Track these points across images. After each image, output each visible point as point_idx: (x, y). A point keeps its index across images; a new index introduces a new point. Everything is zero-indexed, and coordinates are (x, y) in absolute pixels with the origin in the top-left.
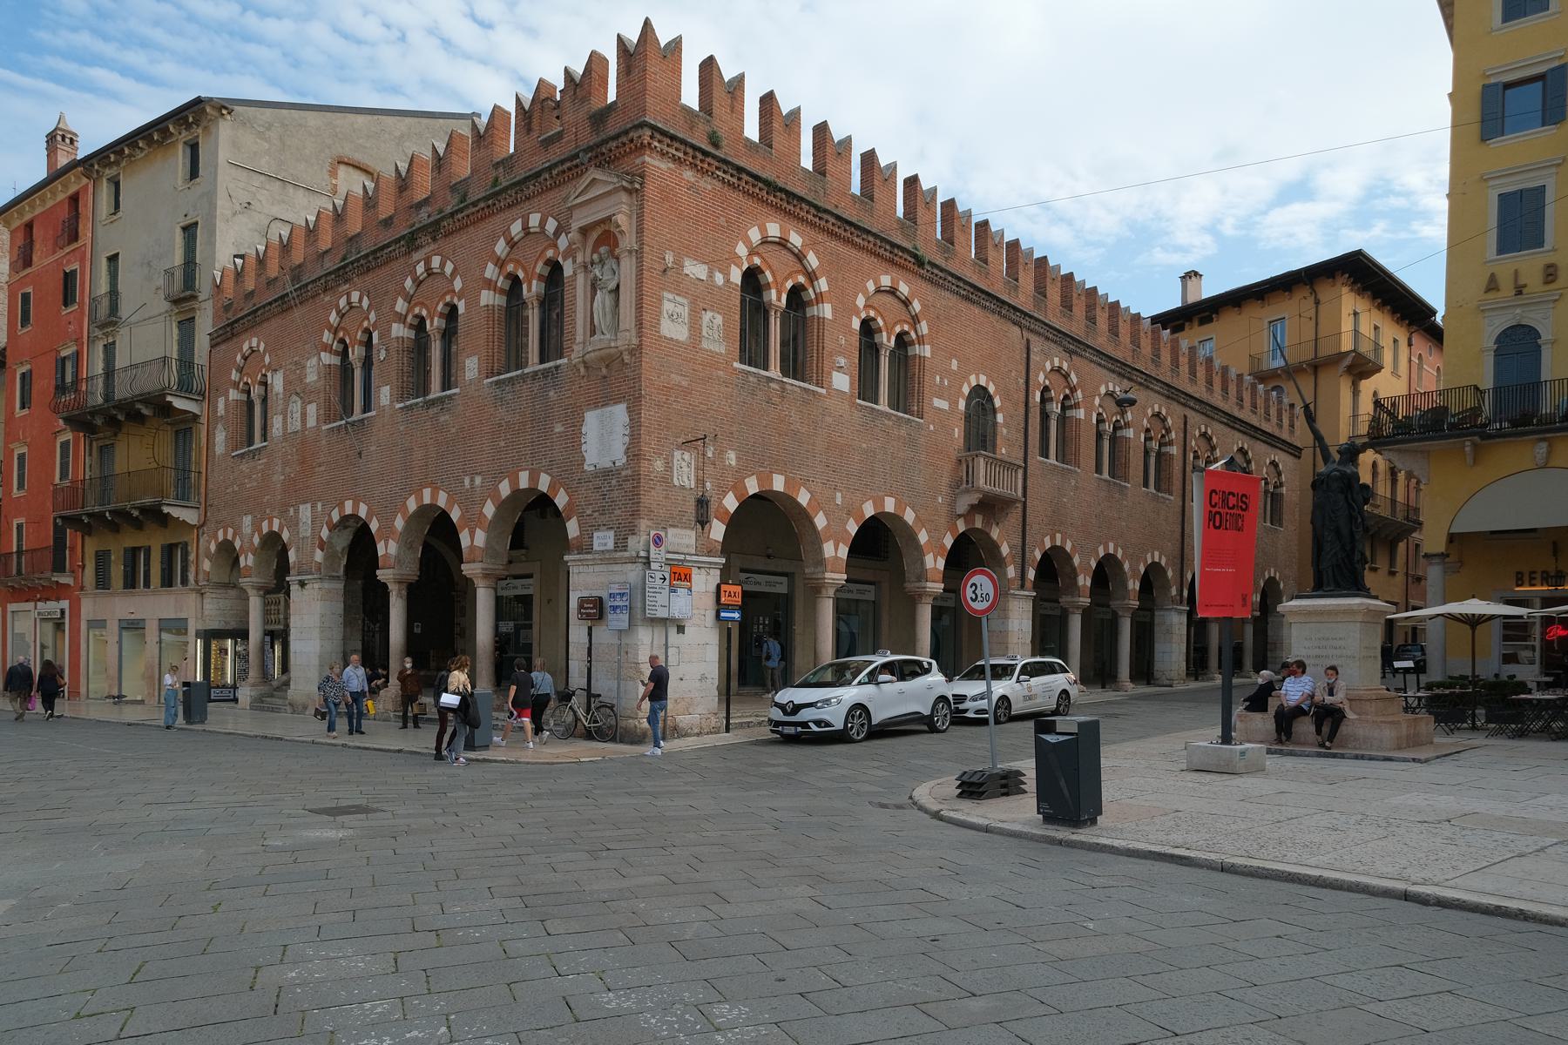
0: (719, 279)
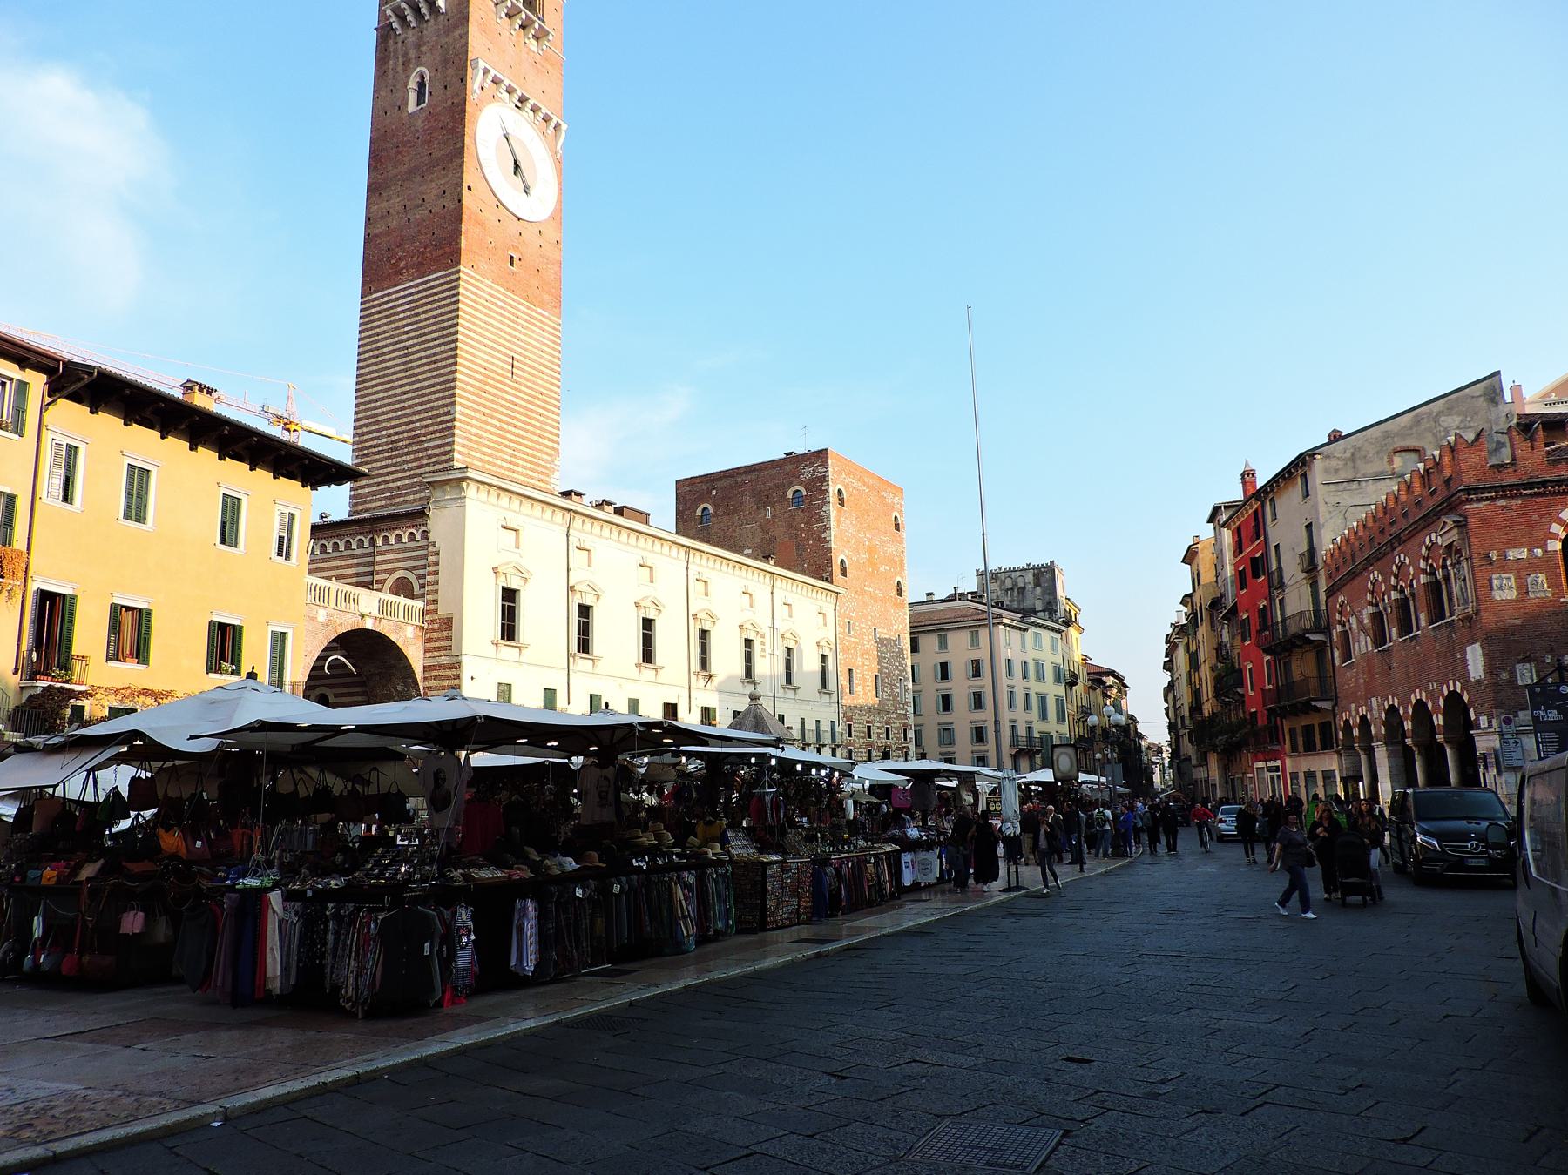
0: (1539, 552)
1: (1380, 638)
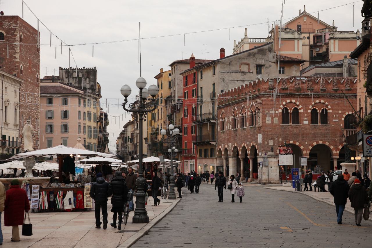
0: (277, 112)
1: (234, 126)
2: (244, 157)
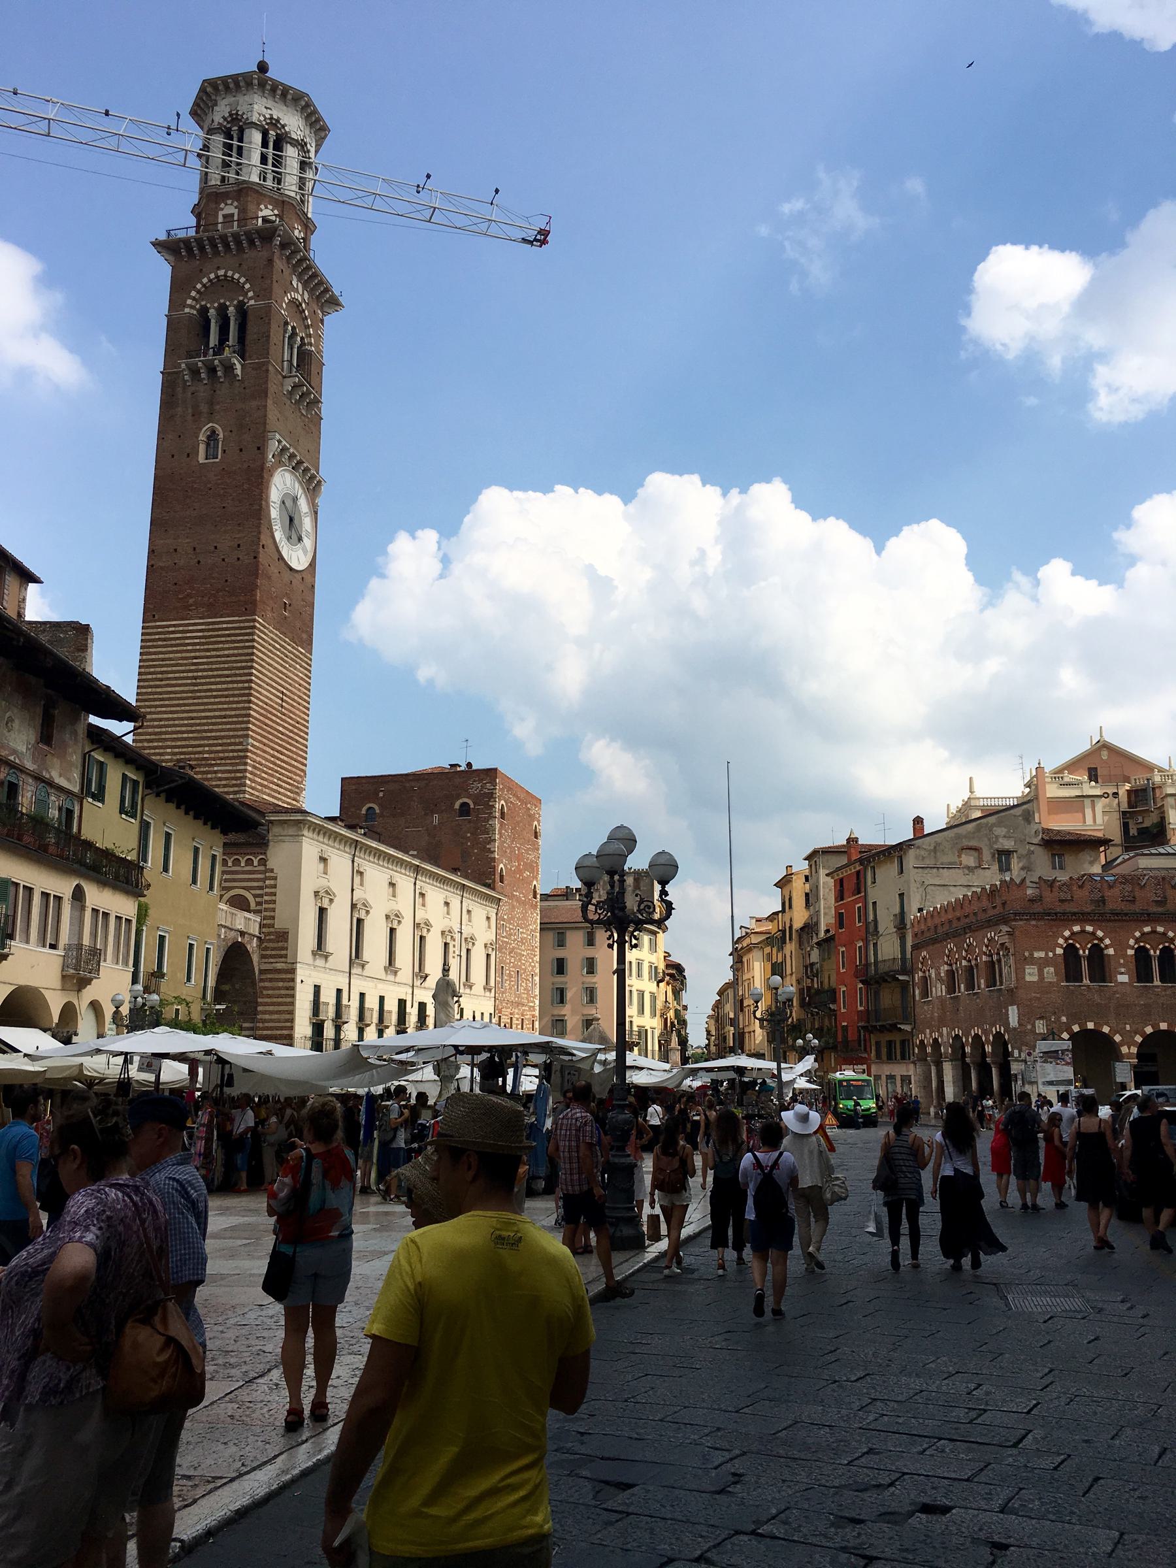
0: (1051, 954)
1: (951, 989)
2: (979, 1060)
